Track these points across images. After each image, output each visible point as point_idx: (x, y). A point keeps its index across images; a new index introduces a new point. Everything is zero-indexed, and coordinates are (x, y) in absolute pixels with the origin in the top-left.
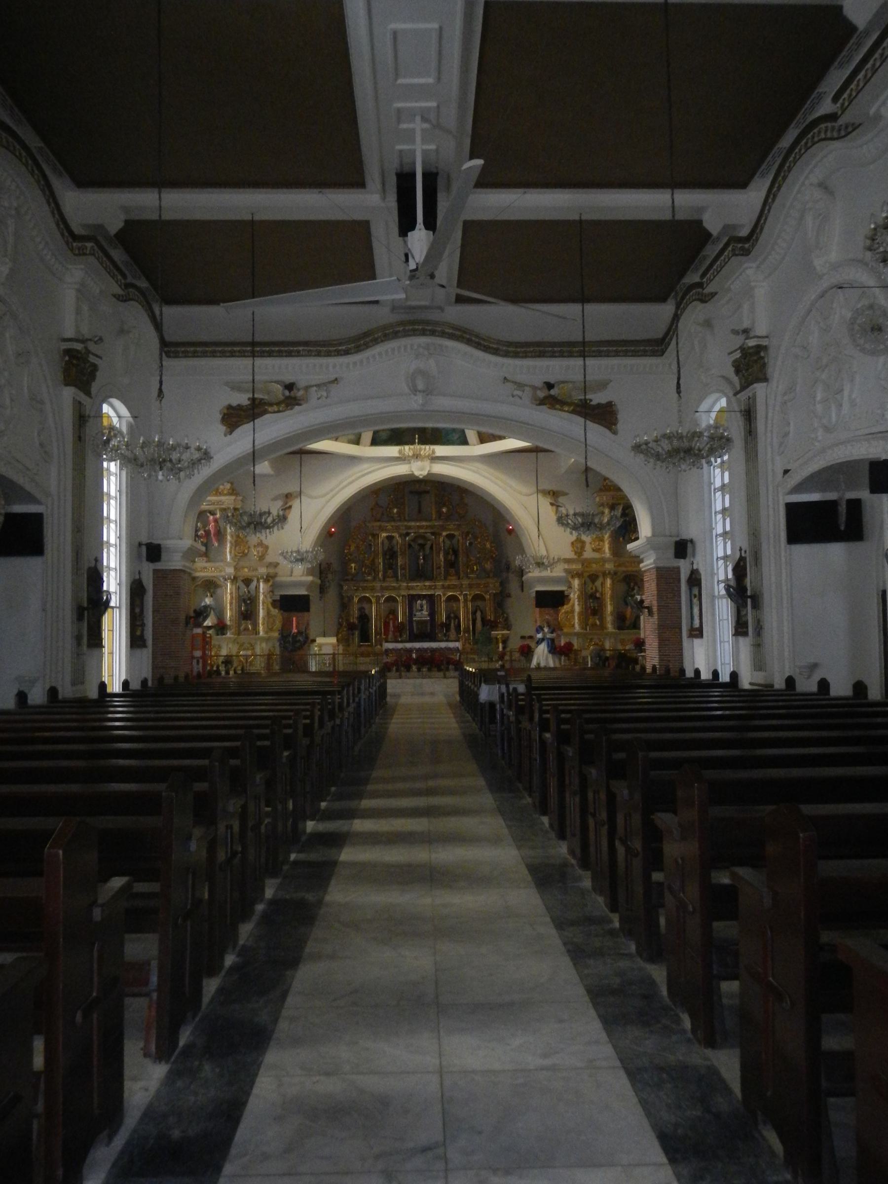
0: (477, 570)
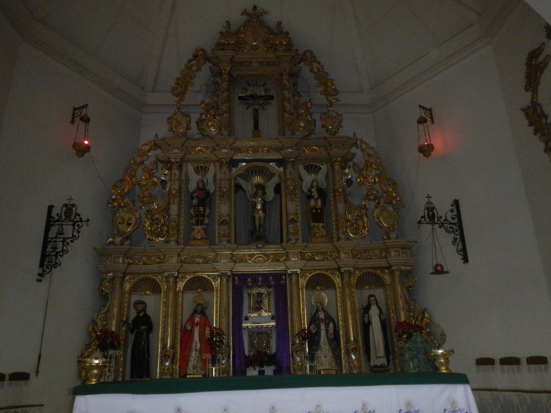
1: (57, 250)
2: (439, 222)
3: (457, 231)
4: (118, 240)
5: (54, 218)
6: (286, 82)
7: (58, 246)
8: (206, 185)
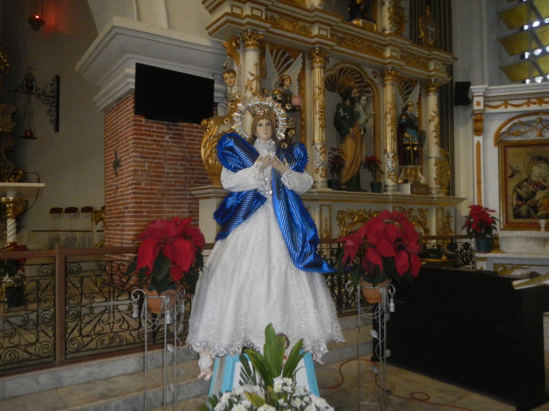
3: (53, 103)
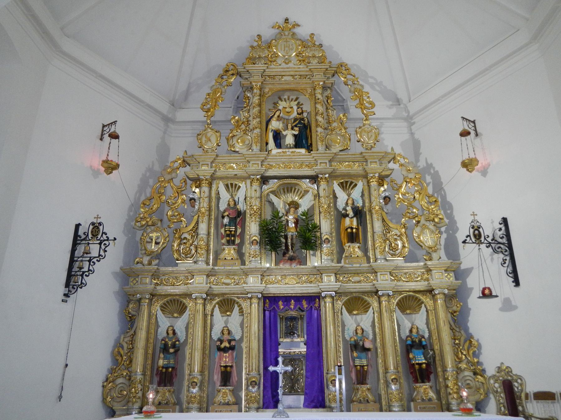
0: (404, 247)
1: (83, 270)
2: (486, 242)
3: (506, 251)
4: (146, 260)
5: (80, 237)
6: (319, 96)
7: (84, 266)
8: (237, 204)
